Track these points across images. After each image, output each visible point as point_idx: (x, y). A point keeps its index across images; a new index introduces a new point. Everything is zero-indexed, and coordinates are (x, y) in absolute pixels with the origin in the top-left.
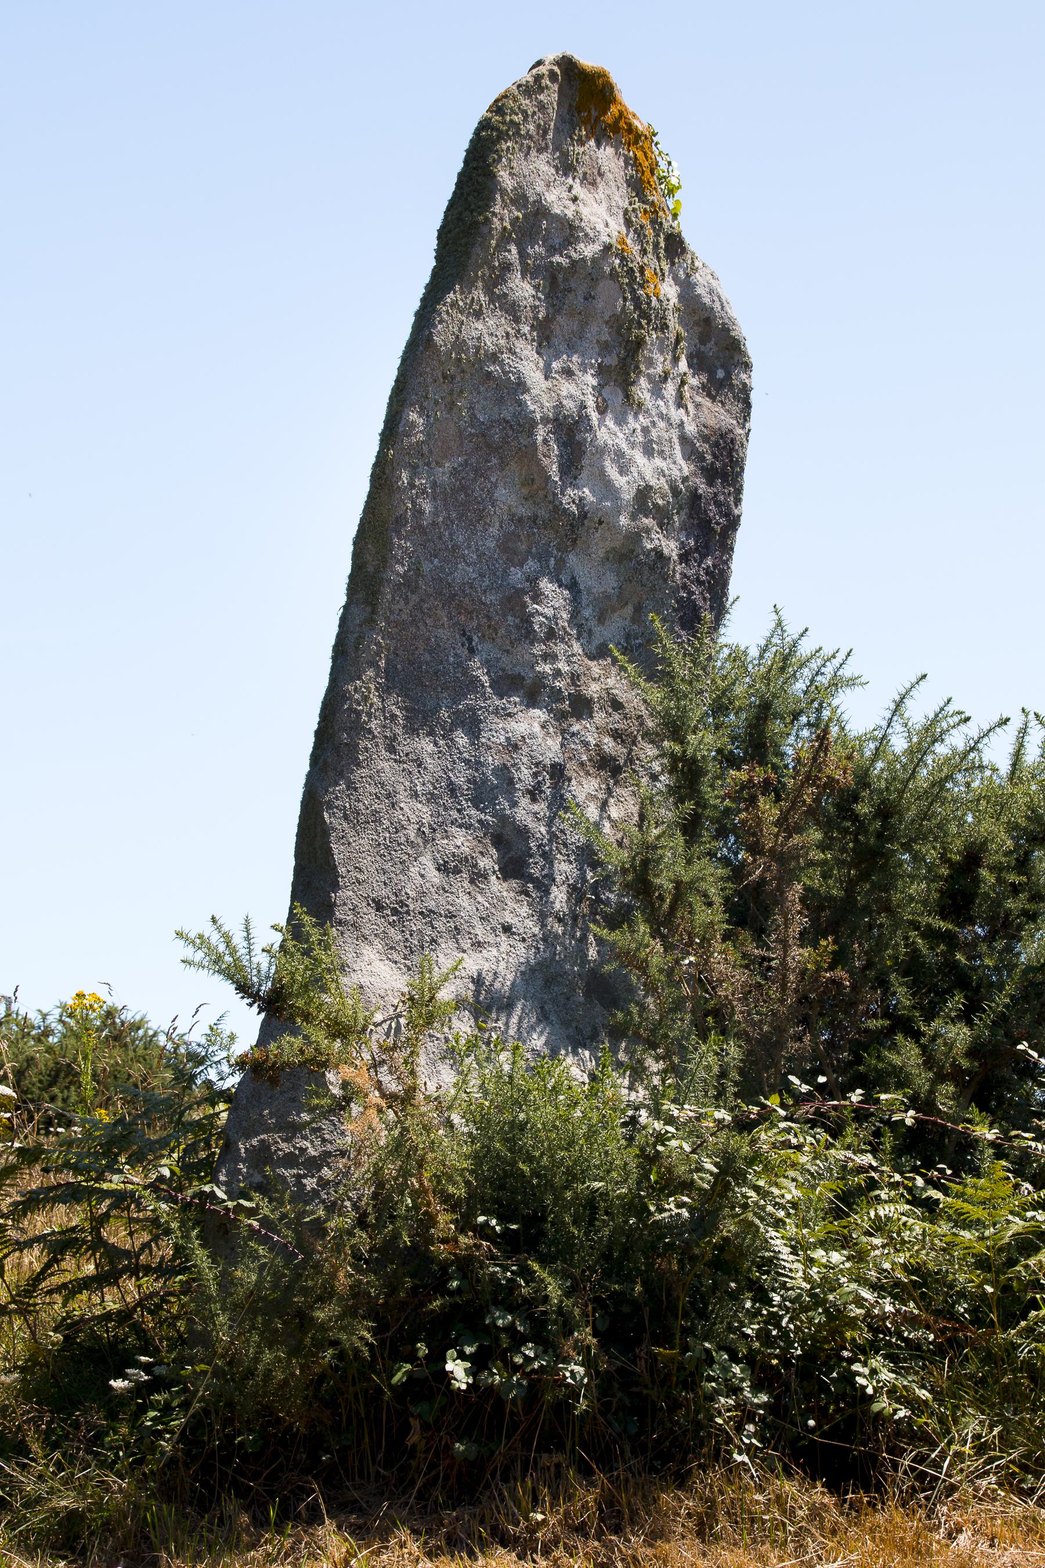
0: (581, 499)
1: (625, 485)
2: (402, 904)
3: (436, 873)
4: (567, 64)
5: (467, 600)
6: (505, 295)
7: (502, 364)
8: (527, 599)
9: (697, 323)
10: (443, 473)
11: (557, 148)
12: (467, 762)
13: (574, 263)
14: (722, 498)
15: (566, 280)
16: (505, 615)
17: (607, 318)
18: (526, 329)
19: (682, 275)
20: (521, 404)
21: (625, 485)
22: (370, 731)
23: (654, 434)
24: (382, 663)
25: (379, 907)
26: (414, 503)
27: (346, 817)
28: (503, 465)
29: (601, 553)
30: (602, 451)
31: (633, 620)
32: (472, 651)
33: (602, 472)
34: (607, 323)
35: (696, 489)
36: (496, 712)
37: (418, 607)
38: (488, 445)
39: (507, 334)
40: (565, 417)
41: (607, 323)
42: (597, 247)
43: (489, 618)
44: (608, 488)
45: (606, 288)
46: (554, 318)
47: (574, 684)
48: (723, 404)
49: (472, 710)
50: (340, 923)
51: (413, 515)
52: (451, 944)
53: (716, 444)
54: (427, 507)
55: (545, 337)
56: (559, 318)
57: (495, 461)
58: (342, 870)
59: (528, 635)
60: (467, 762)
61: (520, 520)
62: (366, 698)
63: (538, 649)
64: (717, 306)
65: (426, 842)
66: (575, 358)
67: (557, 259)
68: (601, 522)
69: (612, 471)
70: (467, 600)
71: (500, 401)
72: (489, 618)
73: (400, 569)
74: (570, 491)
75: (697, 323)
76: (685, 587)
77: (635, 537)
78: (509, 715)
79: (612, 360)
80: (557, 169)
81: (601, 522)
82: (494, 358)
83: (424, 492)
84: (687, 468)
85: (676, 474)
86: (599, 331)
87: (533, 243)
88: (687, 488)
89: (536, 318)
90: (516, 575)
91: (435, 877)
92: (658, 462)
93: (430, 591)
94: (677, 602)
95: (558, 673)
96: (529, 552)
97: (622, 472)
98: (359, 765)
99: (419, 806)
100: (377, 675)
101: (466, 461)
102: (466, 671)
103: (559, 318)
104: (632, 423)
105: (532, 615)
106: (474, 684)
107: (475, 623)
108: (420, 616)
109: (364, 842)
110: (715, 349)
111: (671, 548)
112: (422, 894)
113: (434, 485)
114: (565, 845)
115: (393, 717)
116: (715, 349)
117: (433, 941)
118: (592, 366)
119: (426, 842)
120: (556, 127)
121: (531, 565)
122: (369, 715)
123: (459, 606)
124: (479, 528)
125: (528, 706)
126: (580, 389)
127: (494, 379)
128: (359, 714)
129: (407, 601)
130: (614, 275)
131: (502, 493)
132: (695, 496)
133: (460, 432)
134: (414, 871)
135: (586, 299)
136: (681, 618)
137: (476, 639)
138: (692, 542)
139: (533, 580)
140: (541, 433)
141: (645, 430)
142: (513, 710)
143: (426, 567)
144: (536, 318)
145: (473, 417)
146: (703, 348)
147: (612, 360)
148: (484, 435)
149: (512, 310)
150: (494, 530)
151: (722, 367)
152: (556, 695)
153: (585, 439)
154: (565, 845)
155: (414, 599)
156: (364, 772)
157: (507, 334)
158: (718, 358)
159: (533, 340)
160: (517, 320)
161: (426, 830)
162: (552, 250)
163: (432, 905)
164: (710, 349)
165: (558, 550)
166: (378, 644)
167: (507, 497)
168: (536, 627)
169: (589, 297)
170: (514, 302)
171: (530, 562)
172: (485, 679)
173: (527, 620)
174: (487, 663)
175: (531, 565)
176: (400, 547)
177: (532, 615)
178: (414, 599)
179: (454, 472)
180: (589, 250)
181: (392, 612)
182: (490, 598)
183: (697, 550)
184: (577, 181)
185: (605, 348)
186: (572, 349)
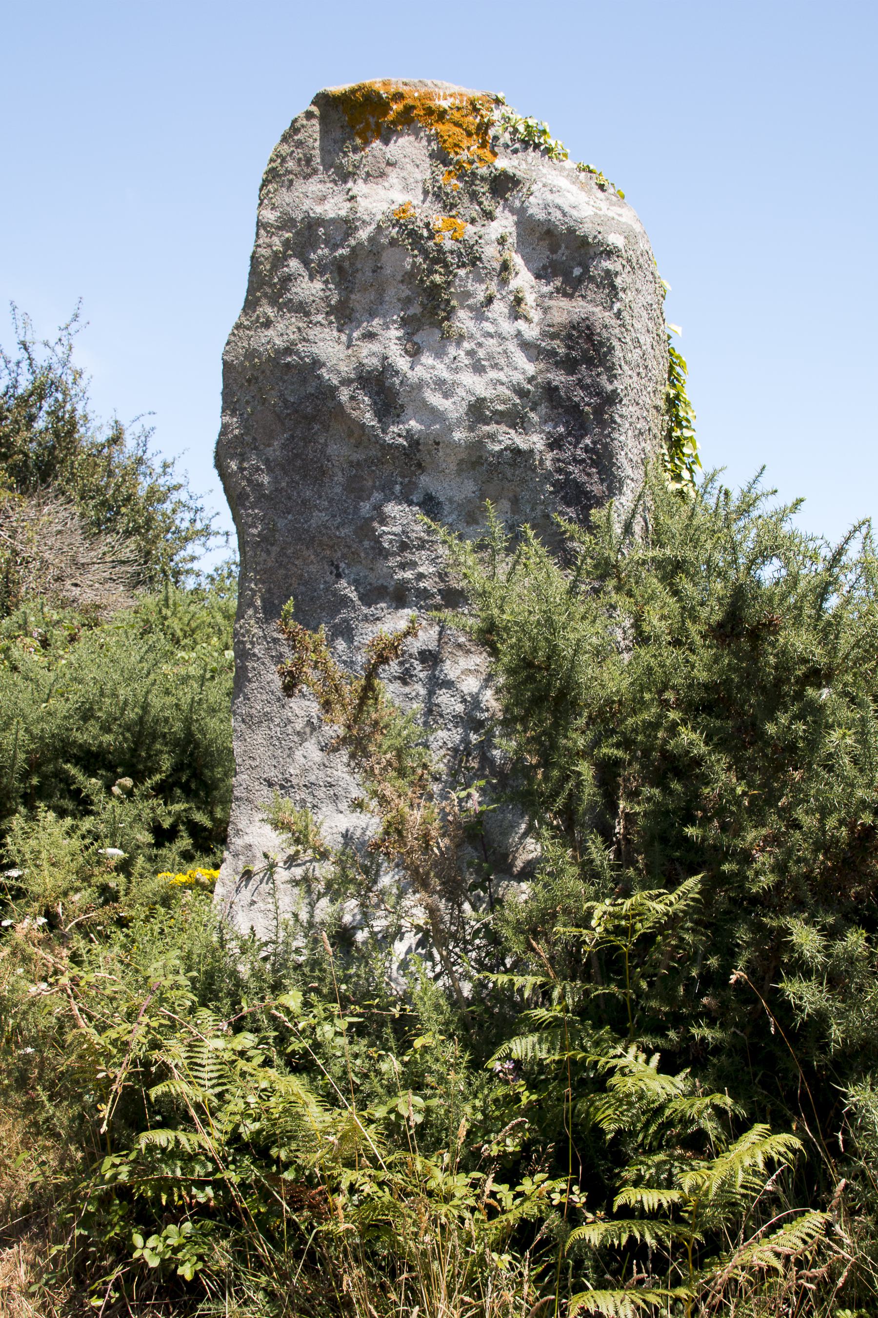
0: (408, 431)
1: (452, 408)
2: (287, 781)
3: (320, 753)
4: (324, 101)
5: (325, 539)
6: (290, 300)
7: (297, 353)
8: (376, 525)
9: (540, 239)
10: (275, 450)
11: (327, 166)
12: (345, 662)
13: (353, 249)
14: (589, 381)
15: (352, 264)
16: (361, 542)
17: (399, 278)
18: (320, 318)
19: (517, 204)
20: (319, 377)
21: (452, 408)
22: (254, 655)
23: (481, 353)
24: (259, 603)
25: (270, 785)
26: (250, 481)
27: (243, 721)
28: (326, 428)
29: (453, 467)
30: (420, 385)
31: (514, 512)
32: (339, 576)
33: (424, 402)
34: (402, 282)
35: (549, 383)
36: (366, 619)
37: (282, 552)
38: (305, 417)
39: (299, 329)
40: (369, 372)
41: (402, 282)
42: (371, 228)
43: (349, 547)
44: (435, 414)
45: (389, 258)
46: (348, 299)
47: (443, 581)
48: (583, 297)
49: (345, 621)
50: (237, 799)
51: (253, 490)
52: (331, 807)
53: (569, 337)
54: (265, 479)
55: (343, 315)
56: (353, 297)
57: (317, 427)
58: (239, 761)
59: (385, 554)
60: (345, 662)
61: (358, 463)
62: (248, 631)
63: (392, 562)
64: (557, 215)
65: (313, 729)
66: (376, 322)
67: (341, 251)
68: (438, 444)
69: (435, 399)
70: (325, 539)
71: (304, 381)
72: (349, 547)
73: (254, 531)
74: (394, 429)
75: (540, 239)
76: (559, 471)
77: (478, 445)
78: (378, 619)
79: (415, 309)
80: (335, 182)
81: (438, 444)
82: (288, 351)
83: (258, 469)
84: (531, 369)
85: (517, 377)
86: (395, 292)
87: (314, 248)
88: (536, 386)
89: (329, 305)
90: (365, 508)
91: (317, 756)
92: (493, 374)
93: (289, 540)
94: (553, 485)
95: (421, 576)
96: (374, 487)
97: (446, 396)
98: (250, 681)
99: (308, 703)
100: (256, 612)
101: (292, 437)
102: (335, 594)
103: (353, 297)
104: (452, 351)
105: (380, 536)
106: (344, 601)
107: (339, 554)
108: (286, 560)
109: (259, 737)
110: (567, 252)
111: (536, 441)
112: (305, 771)
113: (267, 462)
114: (441, 716)
115: (275, 641)
116: (567, 252)
117: (314, 806)
118: (395, 322)
119: (313, 729)
120: (322, 149)
121: (377, 496)
122: (252, 643)
123: (321, 544)
124: (326, 480)
125: (397, 608)
126: (388, 344)
127: (294, 367)
128: (244, 643)
129: (268, 552)
130: (393, 242)
131: (333, 449)
132: (550, 391)
133: (278, 416)
134: (298, 754)
135: (374, 271)
136: (562, 498)
137: (342, 565)
138: (561, 429)
139: (378, 508)
140: (344, 395)
141: (471, 353)
142: (379, 613)
143: (281, 523)
144: (329, 305)
145: (285, 401)
146: (555, 257)
147: (415, 309)
148: (297, 411)
149: (302, 309)
150: (339, 478)
151: (580, 264)
152: (425, 594)
153: (393, 384)
154: (441, 716)
155: (275, 549)
156: (254, 685)
157: (299, 329)
158: (573, 259)
159: (331, 323)
160: (307, 314)
161: (315, 721)
162: (334, 247)
163: (312, 778)
164: (562, 254)
165: (404, 477)
166: (251, 590)
167: (338, 451)
168: (386, 545)
169: (376, 269)
170: (301, 302)
171: (376, 494)
172: (354, 596)
173: (377, 540)
174: (356, 583)
175: (377, 496)
176: (248, 515)
177: (380, 536)
178: (275, 549)
179: (284, 446)
180: (363, 234)
181: (257, 564)
182: (344, 532)
183: (569, 434)
184: (360, 182)
185: (407, 302)
186: (372, 315)
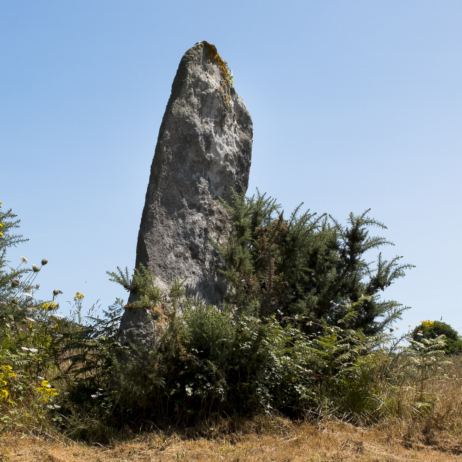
2: (166, 266)
6: (190, 101)
7: (190, 119)
9: (239, 112)
12: (182, 227)
15: (206, 98)
16: (191, 187)
20: (195, 130)
22: (156, 218)
23: (229, 140)
25: (160, 266)
27: (150, 241)
28: (190, 147)
29: (216, 171)
30: (216, 144)
31: (224, 190)
32: (183, 197)
33: (216, 149)
37: (168, 184)
43: (187, 188)
44: (217, 154)
45: (216, 101)
49: (183, 213)
53: (245, 144)
54: (171, 157)
57: (188, 145)
58: (150, 256)
59: (198, 193)
60: (182, 227)
61: (195, 162)
62: (155, 209)
63: (200, 197)
64: (244, 107)
65: (172, 249)
66: (209, 119)
67: (203, 92)
68: (216, 163)
69: (218, 149)
71: (190, 129)
72: (187, 188)
74: (208, 154)
76: (237, 181)
77: (225, 167)
78: (193, 214)
81: (216, 163)
82: (188, 117)
83: (170, 153)
86: (214, 112)
87: (197, 88)
89: (198, 108)
90: (194, 176)
91: (174, 258)
92: (230, 147)
95: (205, 203)
96: (197, 170)
98: (153, 227)
100: (158, 203)
102: (181, 202)
105: (198, 187)
106: (183, 206)
109: (155, 249)
111: (234, 171)
112: (171, 263)
113: (172, 151)
115: (162, 214)
117: (174, 276)
119: (172, 249)
122: (156, 214)
126: (210, 127)
128: (153, 213)
129: (166, 183)
132: (240, 157)
139: (198, 178)
140: (200, 138)
141: (227, 139)
143: (170, 173)
144: (198, 108)
147: (218, 120)
149: (192, 105)
150: (188, 164)
152: (205, 209)
155: (168, 182)
160: (193, 108)
161: (171, 245)
162: (202, 90)
164: (242, 119)
166: (158, 194)
167: (191, 155)
169: (212, 103)
172: (186, 204)
173: (197, 189)
174: (186, 200)
175: (198, 174)
176: (164, 168)
177: (198, 187)
178: (168, 182)
180: (212, 91)
182: (187, 183)
185: (216, 117)
186: (208, 116)
